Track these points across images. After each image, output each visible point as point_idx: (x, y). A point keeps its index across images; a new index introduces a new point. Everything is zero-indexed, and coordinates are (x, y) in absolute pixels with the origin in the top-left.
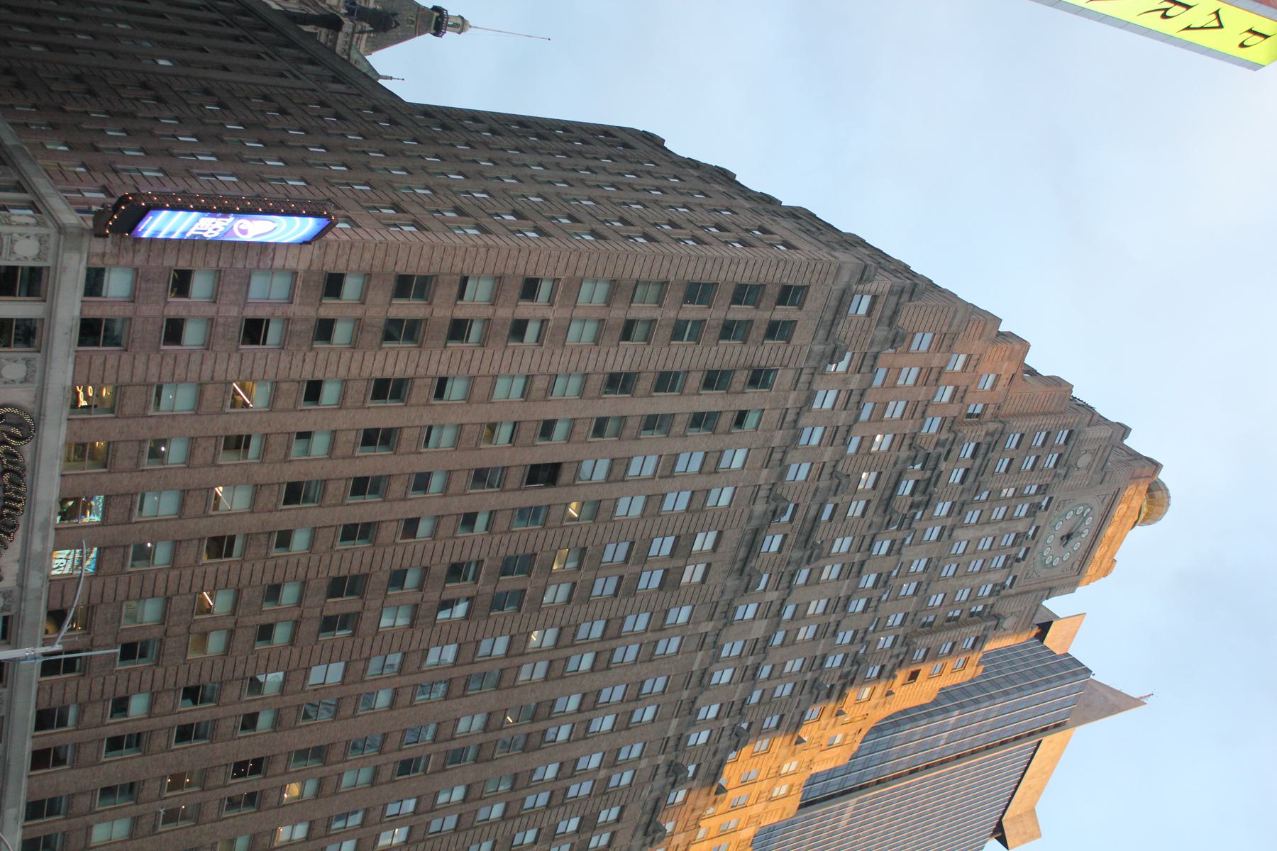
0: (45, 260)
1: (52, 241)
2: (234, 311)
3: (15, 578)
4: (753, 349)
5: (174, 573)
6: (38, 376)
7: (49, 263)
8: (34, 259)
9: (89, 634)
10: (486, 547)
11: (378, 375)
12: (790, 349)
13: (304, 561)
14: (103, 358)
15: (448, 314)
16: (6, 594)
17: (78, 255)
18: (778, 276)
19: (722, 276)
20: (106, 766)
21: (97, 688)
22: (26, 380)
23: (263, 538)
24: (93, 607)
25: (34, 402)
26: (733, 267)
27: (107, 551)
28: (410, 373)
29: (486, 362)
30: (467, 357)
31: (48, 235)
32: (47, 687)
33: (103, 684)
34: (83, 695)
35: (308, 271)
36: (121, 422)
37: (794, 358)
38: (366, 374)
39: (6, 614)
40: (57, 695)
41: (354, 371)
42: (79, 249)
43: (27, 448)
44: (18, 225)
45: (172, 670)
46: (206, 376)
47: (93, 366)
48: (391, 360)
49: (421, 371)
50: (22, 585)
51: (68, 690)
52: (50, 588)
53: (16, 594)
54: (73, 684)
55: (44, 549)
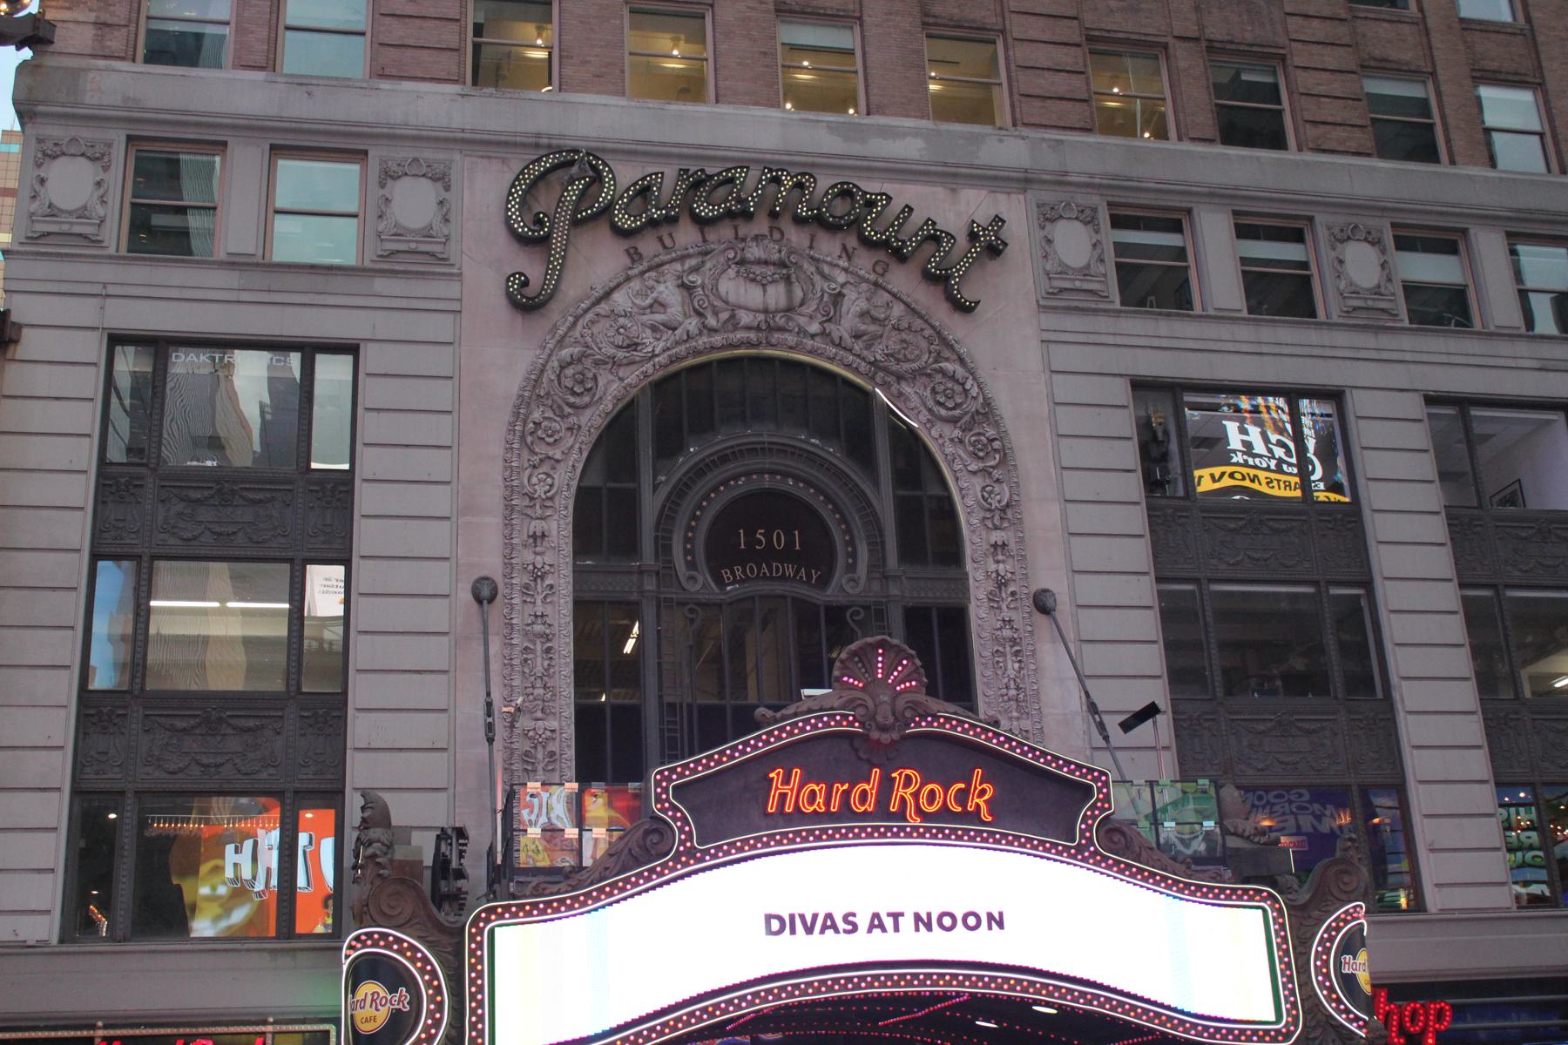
0: (109, 145)
1: (54, 131)
3: (1002, 197)
6: (428, 154)
7: (118, 137)
8: (106, 169)
9: (1165, 47)
14: (388, 20)
16: (1049, 215)
17: (91, 75)
20: (1535, 14)
21: (1318, 30)
22: (442, 179)
24: (1090, 39)
25: (504, 160)
27: (937, 9)
31: (40, 141)
32: (1311, 132)
33: (1306, 16)
39: (1104, 217)
40: (1331, 110)
42: (76, 73)
43: (626, 175)
47: (411, 42)
50: (1024, 181)
51: (1322, 89)
52: (1026, 125)
53: (1048, 196)
54: (1305, 81)
55: (916, 133)
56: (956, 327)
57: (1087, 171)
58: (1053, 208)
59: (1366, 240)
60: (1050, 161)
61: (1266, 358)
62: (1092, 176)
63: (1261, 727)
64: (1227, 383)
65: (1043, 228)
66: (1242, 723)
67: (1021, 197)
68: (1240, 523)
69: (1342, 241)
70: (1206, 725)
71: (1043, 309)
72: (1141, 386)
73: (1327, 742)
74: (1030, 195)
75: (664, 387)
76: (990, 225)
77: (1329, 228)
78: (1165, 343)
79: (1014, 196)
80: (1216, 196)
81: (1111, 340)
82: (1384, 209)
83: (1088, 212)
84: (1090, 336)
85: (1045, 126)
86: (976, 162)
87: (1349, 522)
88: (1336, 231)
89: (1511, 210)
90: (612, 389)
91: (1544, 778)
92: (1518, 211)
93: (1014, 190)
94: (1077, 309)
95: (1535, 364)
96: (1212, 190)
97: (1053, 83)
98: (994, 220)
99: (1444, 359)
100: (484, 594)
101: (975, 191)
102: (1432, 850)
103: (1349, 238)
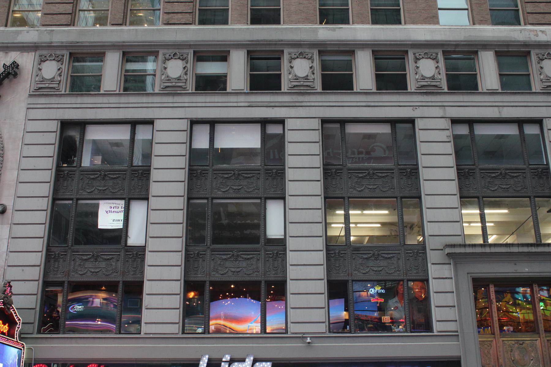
3: (25, 54)
53: (45, 52)
57: (58, 41)
58: (45, 57)
59: (179, 58)
60: (46, 39)
61: (121, 109)
62: (62, 42)
63: (85, 258)
64: (102, 120)
65: (40, 64)
66: (77, 256)
67: (34, 53)
68: (96, 176)
69: (168, 60)
70: (62, 257)
71: (31, 96)
72: (65, 125)
73: (114, 264)
74: (38, 53)
76: (11, 65)
77: (164, 55)
78: (78, 106)
79: (30, 53)
80: (114, 46)
81: (56, 106)
82: (190, 45)
83: (60, 57)
84: (48, 105)
85: (51, 25)
86: (15, 41)
87: (145, 174)
88: (167, 56)
89: (249, 41)
91: (211, 279)
92: (253, 41)
93: (32, 51)
94: (43, 95)
95: (247, 104)
96: (113, 44)
97: (59, 8)
98: (13, 63)
99: (204, 105)
101: (15, 52)
102: (147, 309)
103: (172, 58)
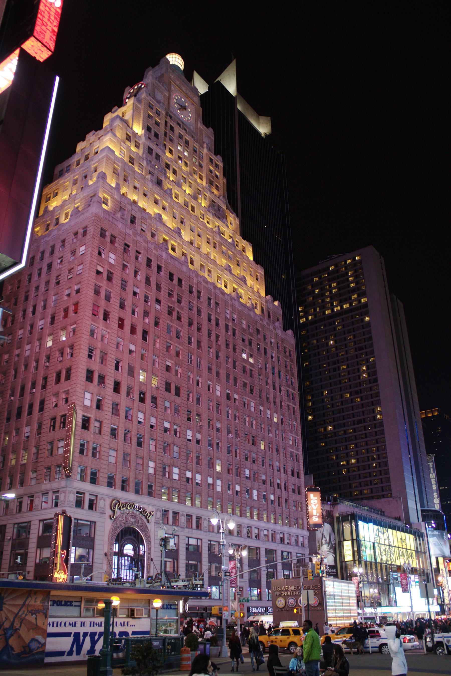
1: (70, 489)
2: (92, 436)
4: (118, 251)
5: (158, 461)
10: (163, 359)
11: (112, 390)
12: (120, 237)
13: (159, 420)
15: (98, 364)
16: (157, 510)
18: (97, 238)
19: (95, 261)
22: (104, 500)
23: (152, 433)
26: (93, 256)
28: (113, 380)
29: (112, 353)
30: (110, 359)
34: (184, 491)
35: (83, 411)
36: (117, 473)
37: (122, 235)
38: (112, 394)
41: (111, 398)
44: (65, 498)
45: (182, 464)
46: (108, 446)
48: (109, 386)
49: (113, 375)
56: (147, 524)
75: (122, 530)
90: (119, 530)
100: (106, 554)
